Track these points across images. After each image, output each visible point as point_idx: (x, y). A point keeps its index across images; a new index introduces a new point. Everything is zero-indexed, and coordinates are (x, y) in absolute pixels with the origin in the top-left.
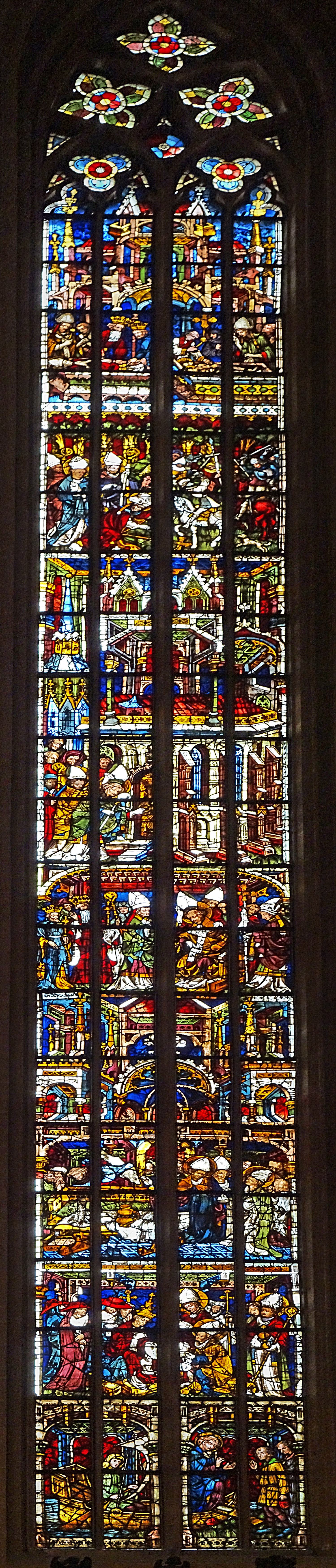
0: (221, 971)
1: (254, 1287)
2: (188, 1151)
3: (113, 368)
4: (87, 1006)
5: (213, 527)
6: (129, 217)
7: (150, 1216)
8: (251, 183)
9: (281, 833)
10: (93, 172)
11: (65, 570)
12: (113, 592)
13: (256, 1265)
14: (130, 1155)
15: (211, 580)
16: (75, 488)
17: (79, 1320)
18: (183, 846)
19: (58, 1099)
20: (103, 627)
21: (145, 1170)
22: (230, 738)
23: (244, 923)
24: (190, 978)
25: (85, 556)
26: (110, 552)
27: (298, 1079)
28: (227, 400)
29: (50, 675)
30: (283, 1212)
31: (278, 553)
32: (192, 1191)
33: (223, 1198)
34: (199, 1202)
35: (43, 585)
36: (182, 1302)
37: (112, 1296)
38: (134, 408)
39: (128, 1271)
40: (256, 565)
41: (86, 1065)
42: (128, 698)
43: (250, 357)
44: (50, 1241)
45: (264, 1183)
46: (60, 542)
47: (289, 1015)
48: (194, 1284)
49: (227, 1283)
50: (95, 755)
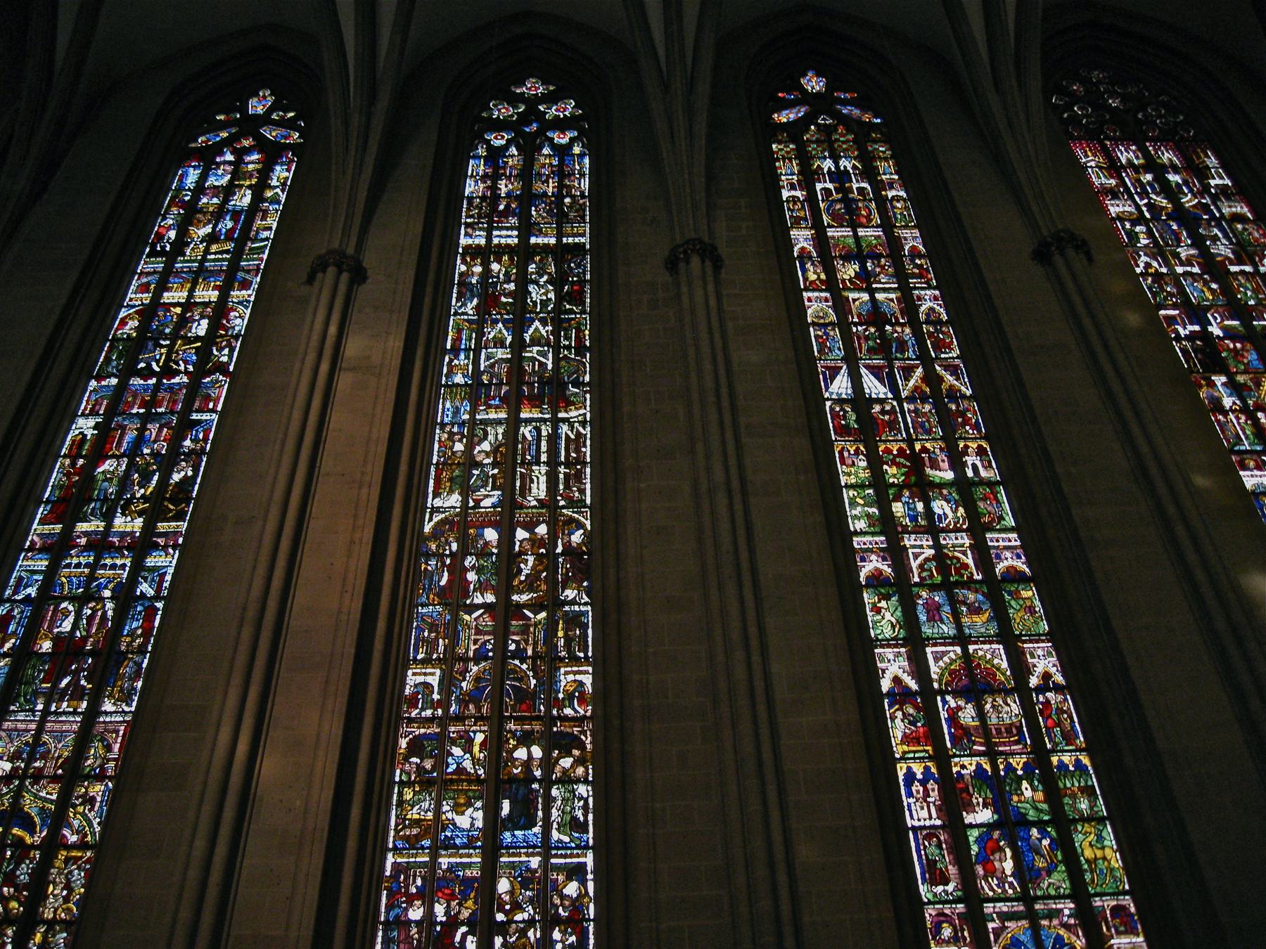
0: (544, 587)
1: (557, 875)
2: (511, 741)
4: (448, 617)
5: (551, 299)
8: (572, 140)
9: (585, 484)
12: (491, 336)
13: (559, 852)
15: (547, 328)
16: (474, 281)
17: (416, 914)
18: (523, 495)
19: (420, 696)
20: (483, 356)
21: (479, 760)
22: (556, 422)
23: (559, 550)
24: (521, 592)
25: (476, 317)
26: (490, 315)
27: (593, 674)
28: (559, 236)
30: (581, 798)
31: (585, 312)
32: (513, 779)
33: (535, 786)
34: (517, 789)
35: (451, 334)
36: (500, 892)
37: (444, 887)
38: (509, 241)
39: (458, 860)
40: (573, 319)
41: (443, 667)
42: (494, 399)
44: (401, 830)
45: (568, 770)
46: (462, 310)
47: (588, 621)
48: (510, 873)
49: (536, 871)
50: (472, 435)
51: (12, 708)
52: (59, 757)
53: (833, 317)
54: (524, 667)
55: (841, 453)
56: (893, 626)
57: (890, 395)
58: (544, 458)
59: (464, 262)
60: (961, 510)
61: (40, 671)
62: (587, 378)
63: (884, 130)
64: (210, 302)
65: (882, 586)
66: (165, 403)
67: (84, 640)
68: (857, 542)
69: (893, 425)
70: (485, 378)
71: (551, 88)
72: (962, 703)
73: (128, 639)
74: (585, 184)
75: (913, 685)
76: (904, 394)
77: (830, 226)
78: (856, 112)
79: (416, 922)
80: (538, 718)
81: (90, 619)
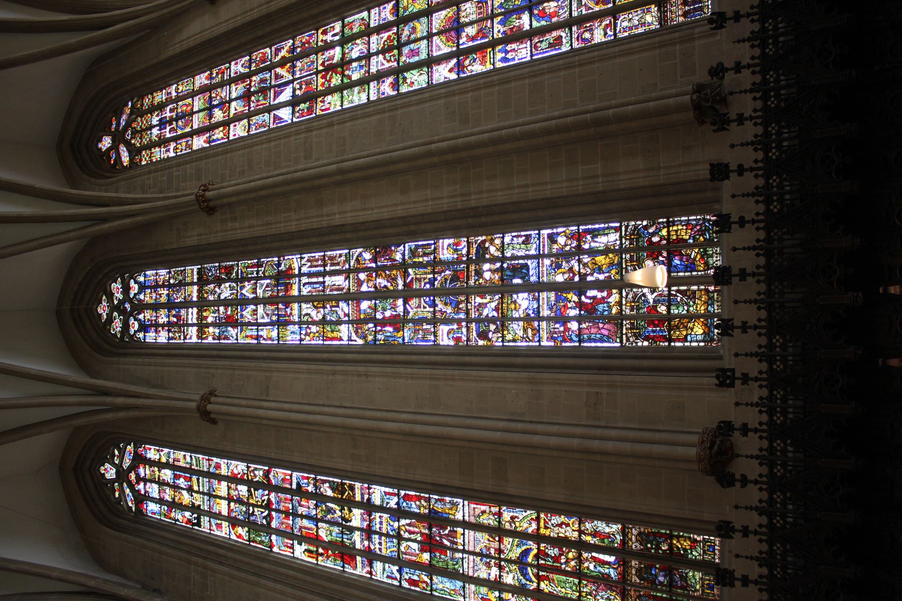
0: (394, 272)
2: (480, 282)
3: (184, 321)
4: (411, 324)
5: (230, 285)
6: (144, 317)
7: (515, 296)
10: (133, 328)
11: (244, 334)
12: (250, 318)
14: (482, 306)
17: (574, 326)
18: (342, 289)
22: (300, 275)
23: (373, 265)
26: (237, 320)
27: (443, 239)
28: (192, 284)
29: (278, 340)
31: (238, 264)
32: (502, 279)
34: (507, 275)
39: (546, 305)
40: (242, 271)
42: (286, 312)
43: (180, 278)
50: (307, 323)
51: (461, 572)
52: (489, 540)
53: (245, 121)
54: (439, 278)
55: (322, 110)
56: (421, 74)
57: (291, 85)
58: (321, 279)
59: (206, 338)
60: (358, 41)
61: (440, 558)
62: (276, 259)
63: (135, 100)
64: (228, 486)
65: (398, 82)
66: (287, 505)
67: (422, 534)
68: (373, 97)
69: (308, 83)
70: (274, 318)
71: (104, 297)
72: (464, 34)
73: (422, 509)
74: (163, 272)
75: (454, 61)
76: (291, 78)
77: (192, 127)
78: (124, 117)
79: (579, 325)
80: (468, 268)
81: (411, 533)
